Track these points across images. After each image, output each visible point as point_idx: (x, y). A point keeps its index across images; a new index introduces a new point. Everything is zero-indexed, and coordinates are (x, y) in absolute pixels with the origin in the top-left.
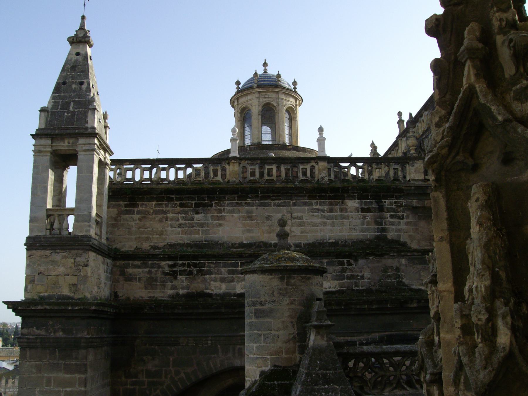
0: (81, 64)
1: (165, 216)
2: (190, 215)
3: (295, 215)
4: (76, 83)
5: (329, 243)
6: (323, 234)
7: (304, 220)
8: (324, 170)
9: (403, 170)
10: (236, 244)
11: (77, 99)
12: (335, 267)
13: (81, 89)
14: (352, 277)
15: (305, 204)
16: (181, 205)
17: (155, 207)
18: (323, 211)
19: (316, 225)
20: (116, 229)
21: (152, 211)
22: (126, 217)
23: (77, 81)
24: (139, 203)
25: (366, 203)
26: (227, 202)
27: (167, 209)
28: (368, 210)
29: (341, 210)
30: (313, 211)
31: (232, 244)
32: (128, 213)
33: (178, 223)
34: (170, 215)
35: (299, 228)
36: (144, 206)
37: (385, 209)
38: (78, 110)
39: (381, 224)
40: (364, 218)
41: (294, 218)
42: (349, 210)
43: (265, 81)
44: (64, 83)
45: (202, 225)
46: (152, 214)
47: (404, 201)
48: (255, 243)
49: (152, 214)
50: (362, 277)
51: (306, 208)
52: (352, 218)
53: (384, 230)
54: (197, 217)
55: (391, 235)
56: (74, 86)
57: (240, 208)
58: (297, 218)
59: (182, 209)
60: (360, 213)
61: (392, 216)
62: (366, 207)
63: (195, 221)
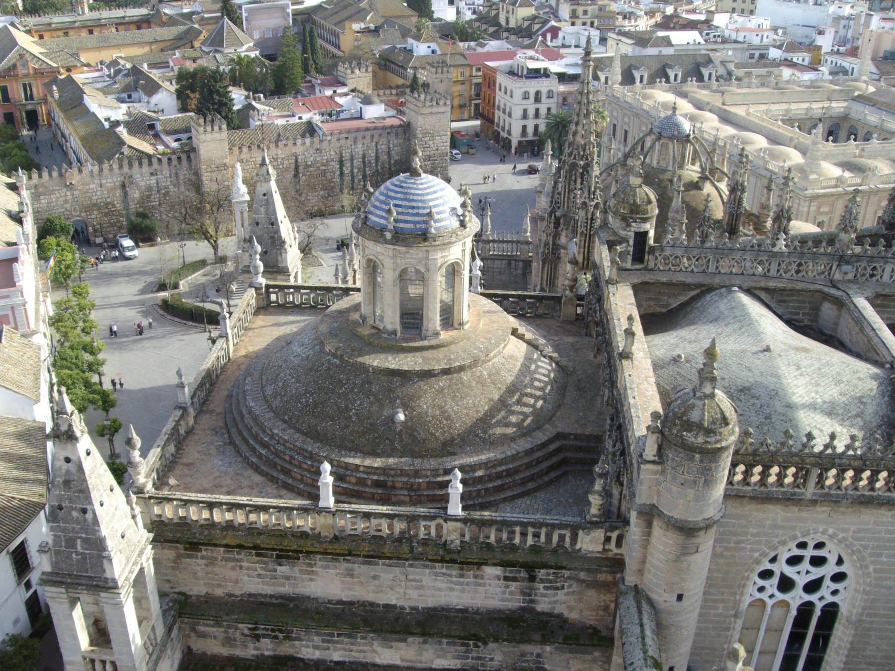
3: (410, 577)
6: (447, 599)
8: (455, 531)
9: (574, 538)
12: (457, 648)
14: (479, 658)
19: (439, 590)
25: (511, 572)
28: (514, 579)
29: (475, 577)
30: (436, 575)
37: (538, 580)
39: (530, 595)
41: (410, 581)
42: (486, 577)
43: (406, 222)
47: (567, 573)
48: (358, 602)
50: (492, 660)
51: (427, 571)
58: (414, 580)
60: (502, 581)
61: (546, 588)
62: (511, 575)
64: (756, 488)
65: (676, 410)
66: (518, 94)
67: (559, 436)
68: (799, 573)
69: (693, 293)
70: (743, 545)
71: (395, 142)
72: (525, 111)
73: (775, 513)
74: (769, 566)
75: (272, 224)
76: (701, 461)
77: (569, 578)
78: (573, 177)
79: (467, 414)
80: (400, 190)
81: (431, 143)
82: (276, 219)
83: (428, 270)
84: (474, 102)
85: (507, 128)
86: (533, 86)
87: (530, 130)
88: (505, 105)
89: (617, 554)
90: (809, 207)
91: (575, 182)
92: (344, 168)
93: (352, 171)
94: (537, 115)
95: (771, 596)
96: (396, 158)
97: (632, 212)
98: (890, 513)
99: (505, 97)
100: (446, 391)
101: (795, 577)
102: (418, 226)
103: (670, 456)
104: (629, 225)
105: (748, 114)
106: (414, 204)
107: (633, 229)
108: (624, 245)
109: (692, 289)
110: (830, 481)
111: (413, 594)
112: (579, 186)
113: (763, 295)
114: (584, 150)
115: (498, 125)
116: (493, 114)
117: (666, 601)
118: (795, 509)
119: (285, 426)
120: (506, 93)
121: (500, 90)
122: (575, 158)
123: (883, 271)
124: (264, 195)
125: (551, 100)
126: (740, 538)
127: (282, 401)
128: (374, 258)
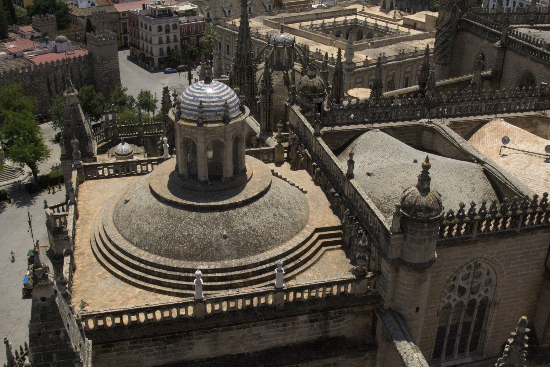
0: (51, 311)
1: (140, 349)
2: (162, 346)
4: (51, 332)
5: (281, 347)
7: (262, 335)
10: (204, 359)
11: (58, 350)
13: (59, 339)
15: (263, 324)
16: (153, 340)
17: (130, 344)
18: (278, 327)
20: (97, 364)
21: (127, 348)
22: (105, 355)
23: (53, 330)
24: (115, 344)
26: (194, 333)
27: (141, 344)
29: (293, 324)
31: (201, 360)
32: (107, 352)
33: (152, 352)
34: (145, 348)
35: (257, 341)
36: (120, 345)
38: (63, 361)
40: (312, 326)
44: (40, 334)
45: (173, 351)
46: (128, 350)
47: (346, 310)
49: (128, 350)
51: (264, 327)
52: (302, 327)
53: (327, 332)
54: (168, 346)
55: (332, 334)
56: (50, 336)
57: (207, 335)
59: (155, 342)
60: (309, 323)
61: (335, 322)
62: (314, 318)
63: (168, 349)
64: (447, 239)
65: (410, 200)
66: (155, 28)
67: (317, 230)
68: (468, 283)
69: (352, 136)
70: (441, 273)
71: (83, 66)
72: (160, 39)
73: (457, 251)
74: (452, 283)
75: (79, 125)
76: (428, 228)
77: (348, 313)
78: (242, 76)
79: (264, 226)
80: (202, 91)
81: (107, 65)
82: (82, 121)
83: (226, 140)
84: (123, 36)
85: (149, 50)
86: (163, 22)
87: (165, 50)
88: (147, 36)
89: (374, 293)
90: (351, 80)
91: (244, 79)
92: (51, 87)
93: (56, 87)
94: (168, 41)
95: (455, 300)
96: (85, 77)
97: (313, 92)
98: (514, 240)
99: (146, 31)
100: (248, 214)
101: (466, 287)
102: (218, 113)
103: (409, 228)
104: (312, 100)
105: (300, 26)
106: (214, 100)
107: (314, 102)
108: (310, 112)
109: (352, 134)
110: (483, 228)
111: (255, 343)
112: (246, 81)
113: (391, 131)
114: (248, 58)
115: (143, 50)
116: (139, 42)
117: (410, 314)
118: (467, 247)
119: (147, 253)
120: (146, 28)
121: (142, 27)
122: (243, 64)
123: (451, 110)
124: (72, 106)
125: (176, 31)
126: (439, 269)
127: (139, 238)
128: (190, 137)
